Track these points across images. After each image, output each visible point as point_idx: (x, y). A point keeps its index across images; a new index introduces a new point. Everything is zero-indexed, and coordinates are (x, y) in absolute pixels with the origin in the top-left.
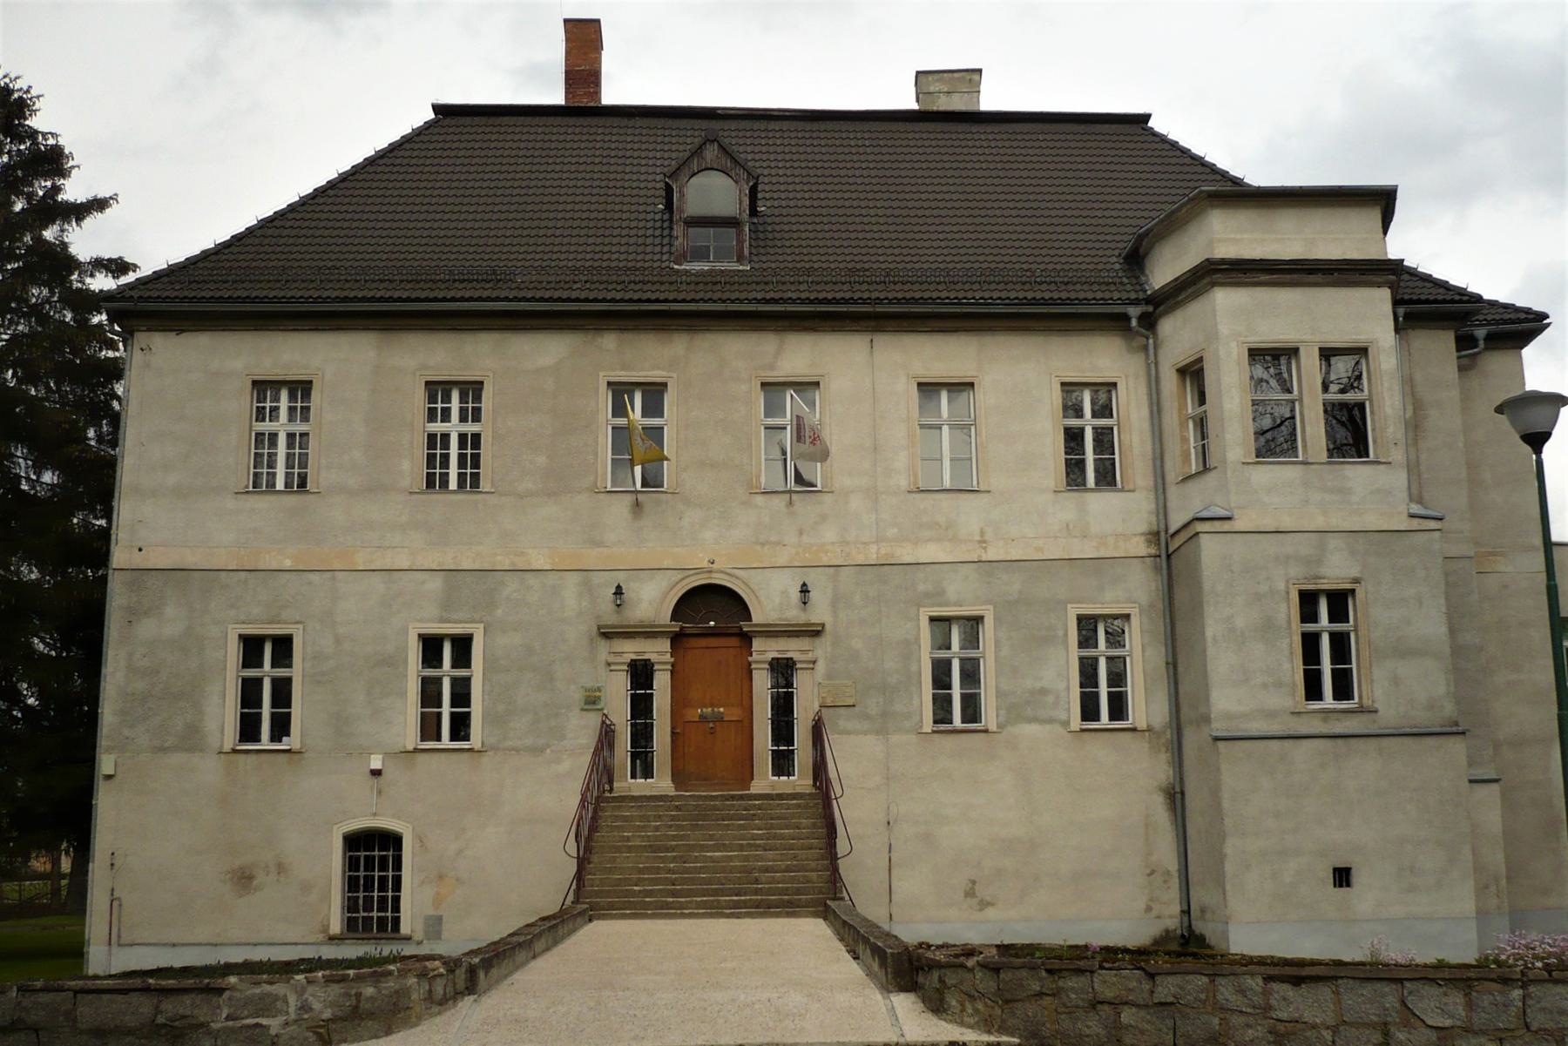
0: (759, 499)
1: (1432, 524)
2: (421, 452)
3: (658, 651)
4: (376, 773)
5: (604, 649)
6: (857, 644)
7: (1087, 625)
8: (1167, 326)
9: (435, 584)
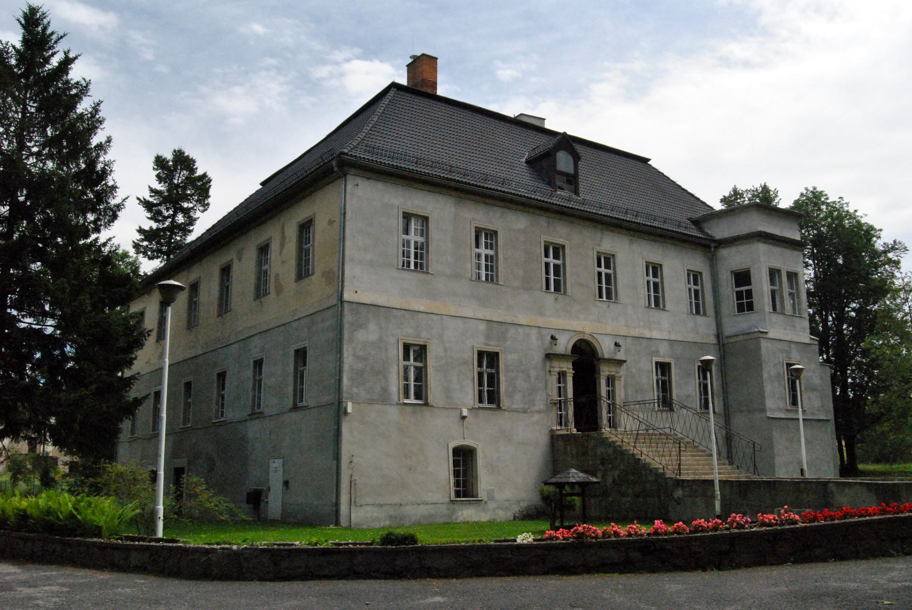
3: (567, 367)
4: (464, 418)
6: (634, 370)
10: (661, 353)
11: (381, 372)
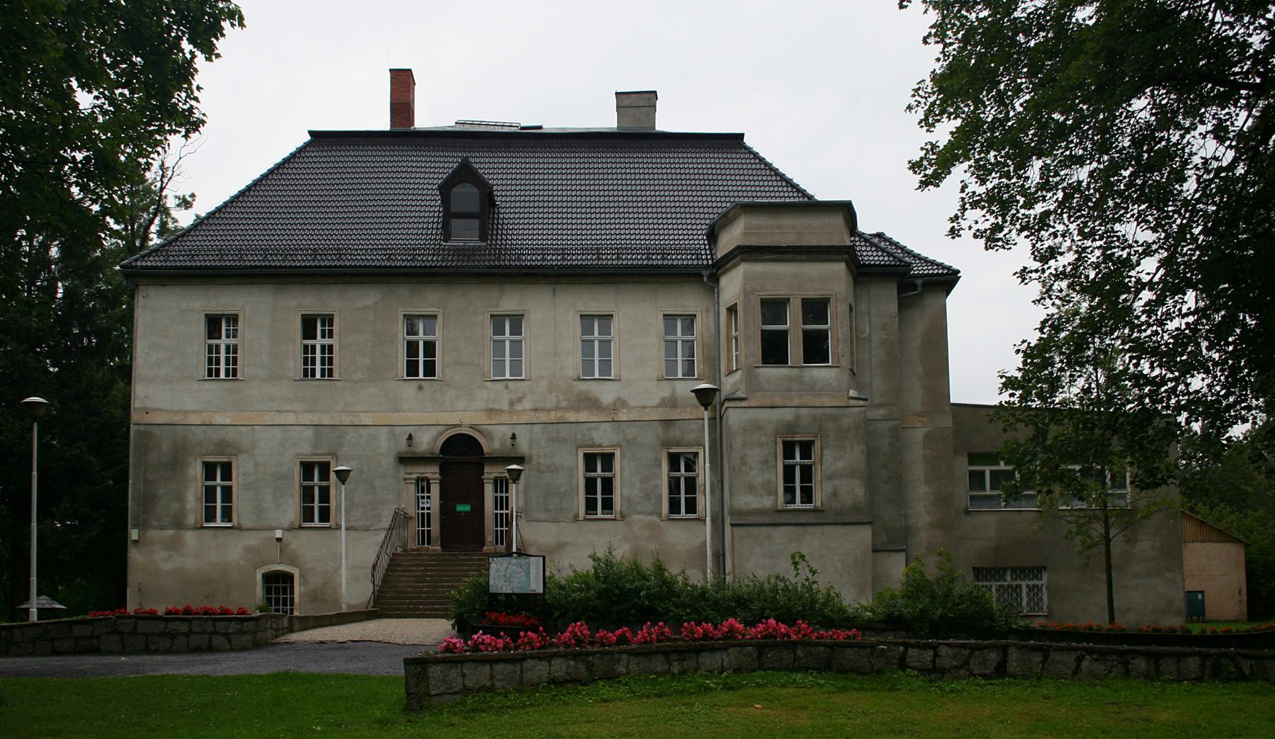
0: (489, 384)
1: (861, 403)
2: (300, 356)
3: (432, 472)
4: (279, 540)
5: (403, 471)
8: (724, 281)
9: (309, 433)
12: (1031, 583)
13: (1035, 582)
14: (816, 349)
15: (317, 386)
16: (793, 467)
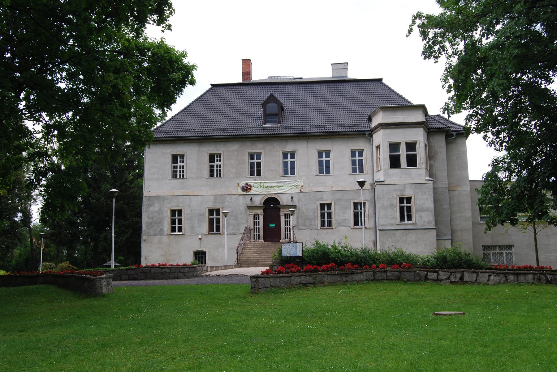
2: (208, 169)
3: (260, 212)
4: (200, 239)
5: (249, 212)
6: (304, 209)
7: (356, 205)
8: (374, 136)
9: (212, 198)
10: (325, 198)
11: (160, 222)
12: (507, 252)
13: (509, 251)
14: (412, 161)
15: (215, 180)
16: (403, 207)
